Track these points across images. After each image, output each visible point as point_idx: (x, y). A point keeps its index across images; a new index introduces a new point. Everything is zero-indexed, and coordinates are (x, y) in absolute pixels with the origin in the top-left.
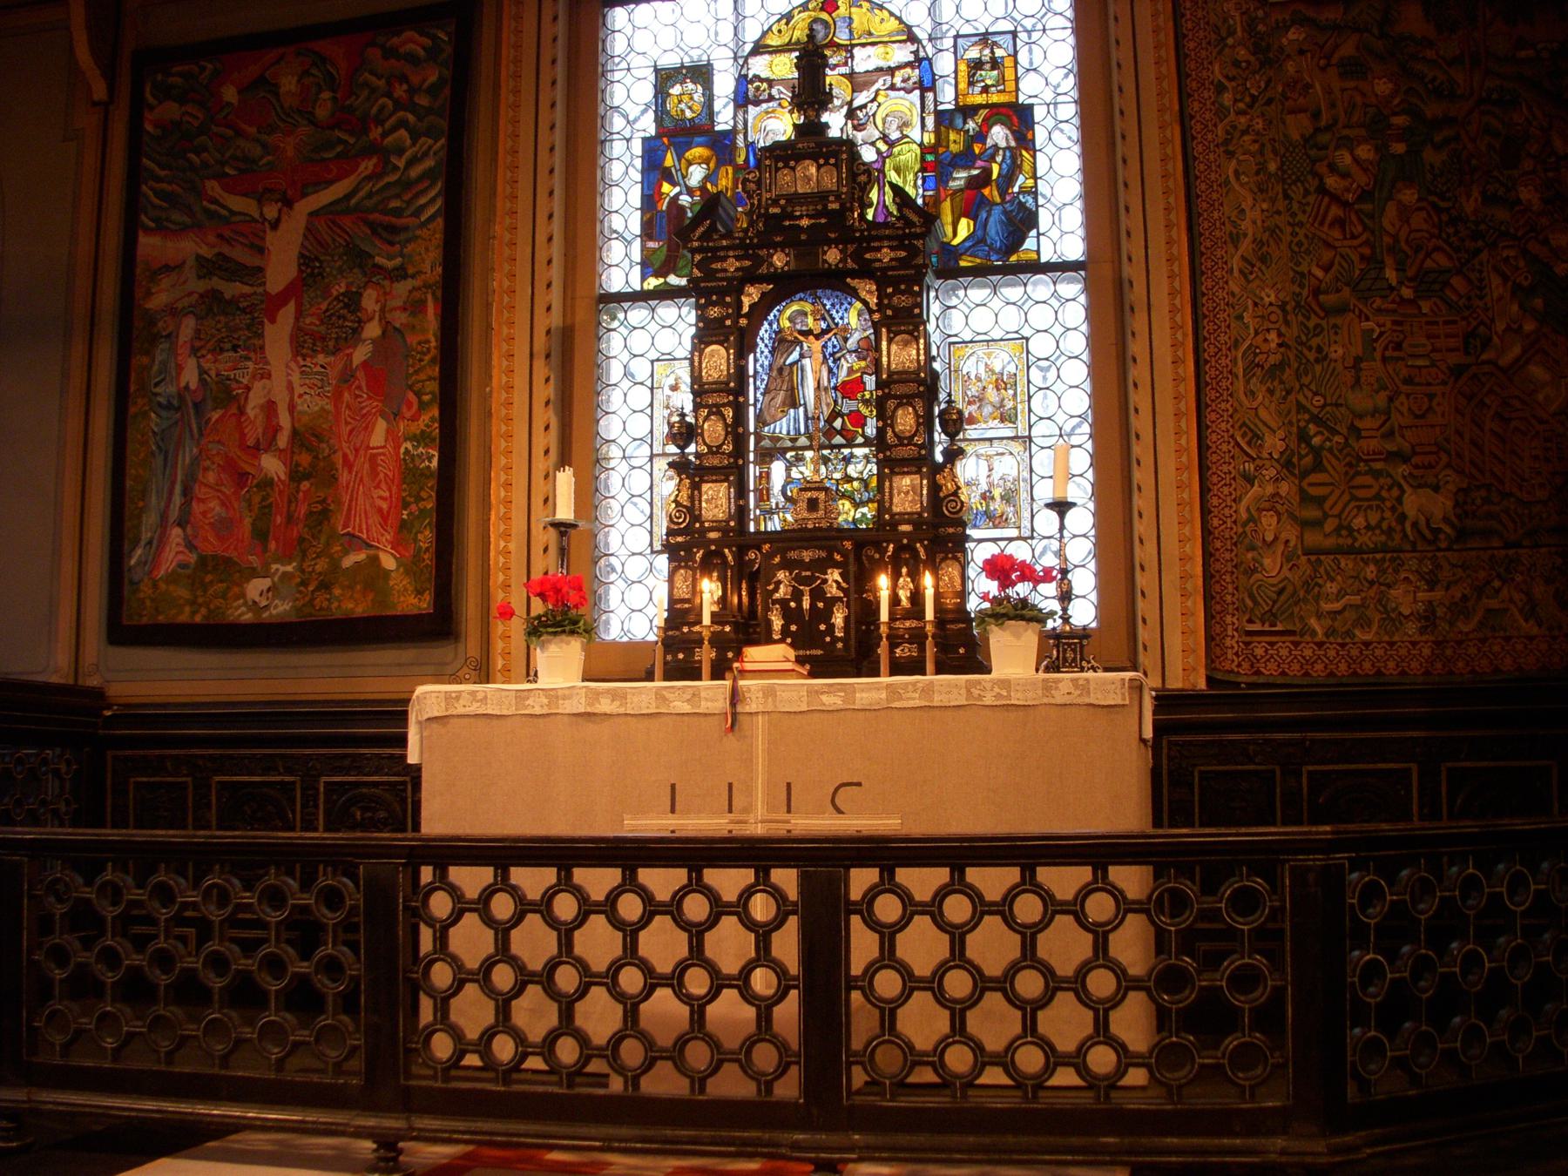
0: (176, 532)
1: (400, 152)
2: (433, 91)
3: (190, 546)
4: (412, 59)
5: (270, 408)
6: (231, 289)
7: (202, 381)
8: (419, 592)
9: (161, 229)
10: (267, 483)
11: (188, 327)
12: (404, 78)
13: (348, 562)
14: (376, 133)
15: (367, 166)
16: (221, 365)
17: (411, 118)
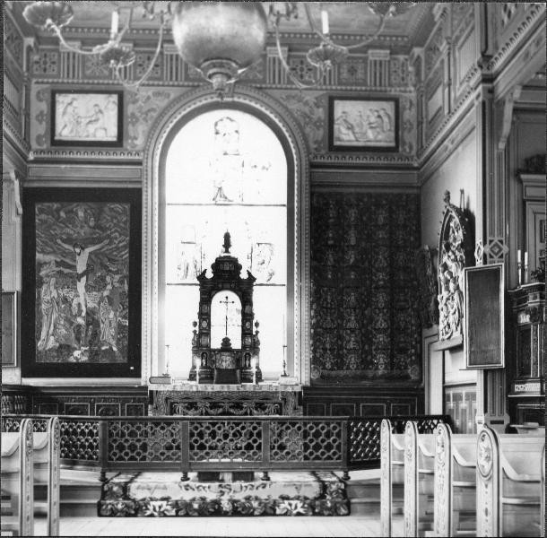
0: (52, 338)
1: (116, 238)
2: (125, 223)
3: (57, 341)
4: (117, 212)
5: (79, 305)
6: (66, 271)
7: (59, 296)
8: (124, 358)
9: (43, 252)
10: (79, 326)
11: (53, 281)
12: (116, 218)
13: (103, 348)
14: (109, 232)
15: (107, 241)
16: (64, 292)
17: (119, 230)
